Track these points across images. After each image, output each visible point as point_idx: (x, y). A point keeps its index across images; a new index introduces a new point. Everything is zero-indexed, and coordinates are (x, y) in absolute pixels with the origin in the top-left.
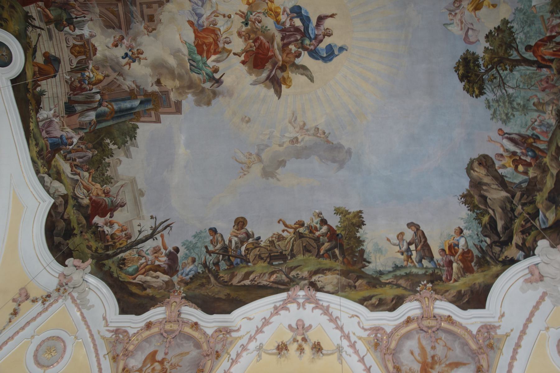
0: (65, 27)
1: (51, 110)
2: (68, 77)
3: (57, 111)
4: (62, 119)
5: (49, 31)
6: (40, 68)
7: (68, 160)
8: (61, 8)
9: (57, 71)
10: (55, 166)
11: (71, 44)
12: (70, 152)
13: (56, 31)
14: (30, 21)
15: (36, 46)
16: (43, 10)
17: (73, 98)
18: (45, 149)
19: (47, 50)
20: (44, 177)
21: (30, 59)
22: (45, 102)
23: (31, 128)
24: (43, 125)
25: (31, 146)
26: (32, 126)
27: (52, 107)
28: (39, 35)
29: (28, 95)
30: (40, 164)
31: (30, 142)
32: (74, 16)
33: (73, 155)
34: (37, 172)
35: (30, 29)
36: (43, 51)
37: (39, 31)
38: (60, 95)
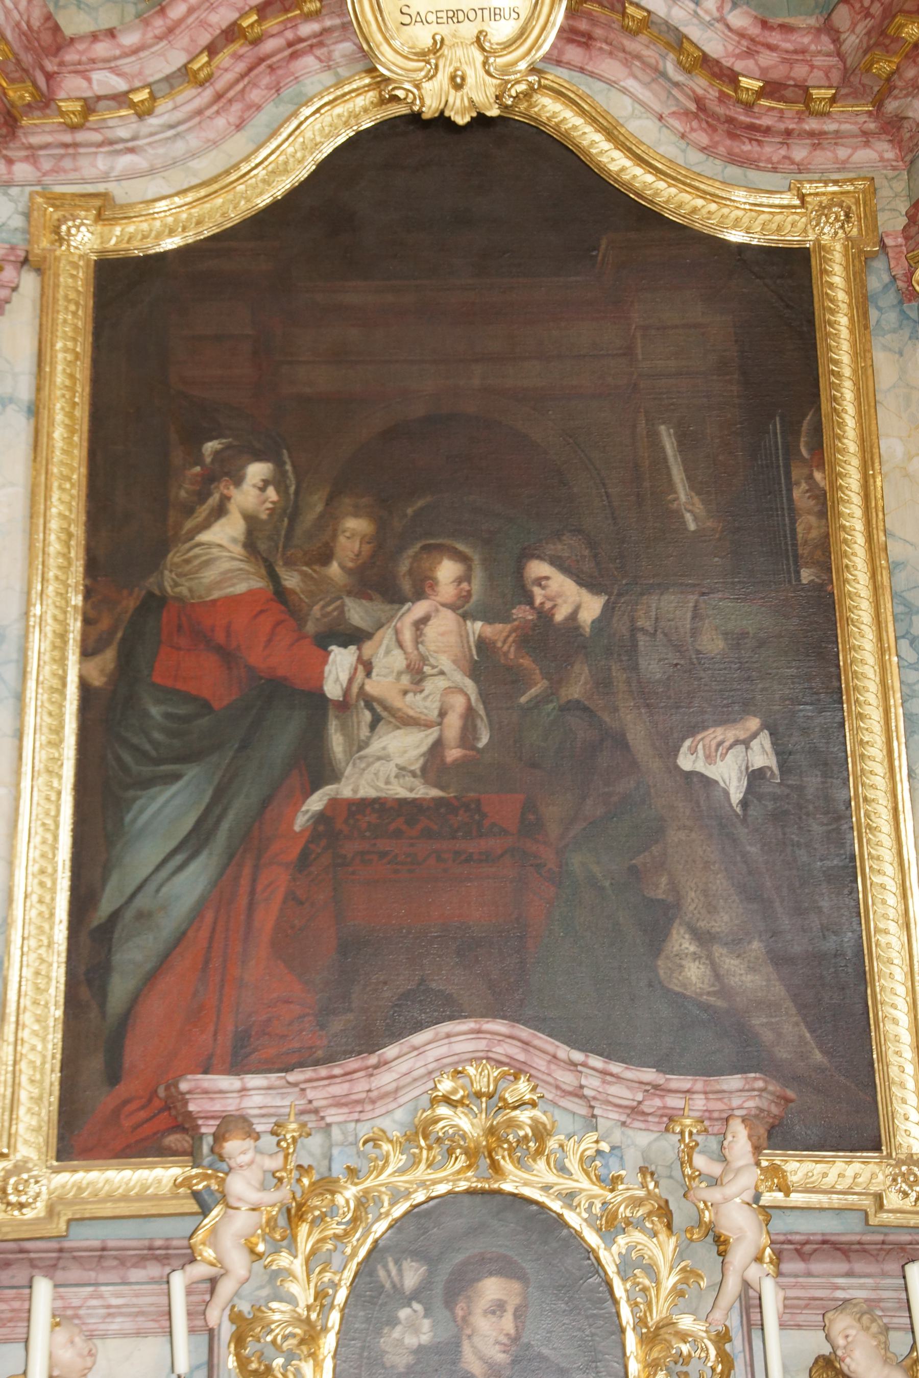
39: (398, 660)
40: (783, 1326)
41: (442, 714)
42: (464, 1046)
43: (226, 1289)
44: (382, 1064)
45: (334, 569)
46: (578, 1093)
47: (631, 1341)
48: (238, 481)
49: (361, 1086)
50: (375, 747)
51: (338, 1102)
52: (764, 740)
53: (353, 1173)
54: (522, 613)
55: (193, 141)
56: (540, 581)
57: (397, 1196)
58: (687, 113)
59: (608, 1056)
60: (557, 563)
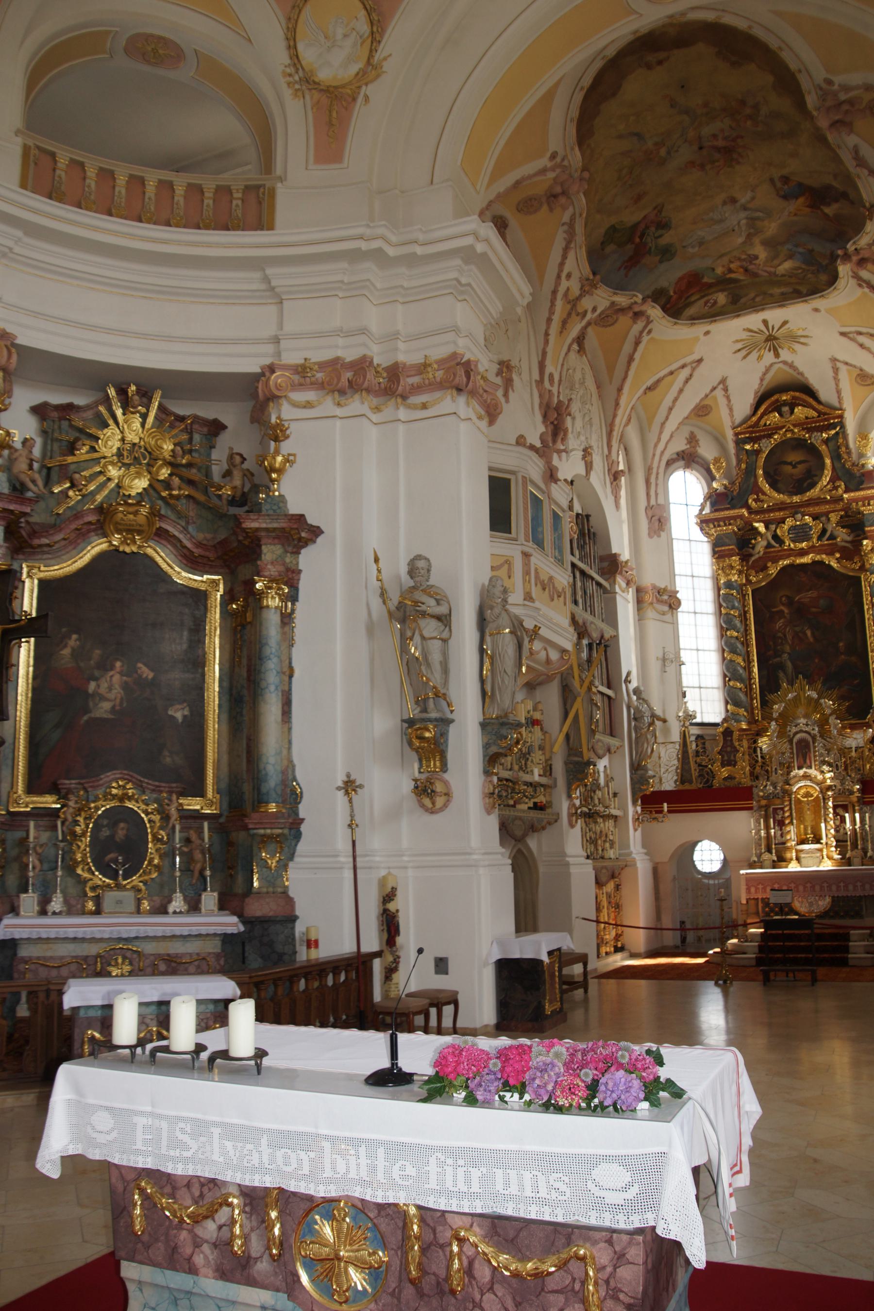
39: (106, 685)
40: (180, 832)
41: (115, 699)
42: (118, 776)
43: (67, 823)
44: (101, 779)
45: (92, 662)
46: (142, 786)
47: (150, 837)
48: (70, 638)
49: (96, 784)
50: (100, 705)
51: (91, 787)
52: (187, 708)
53: (94, 802)
54: (135, 675)
55: (63, 552)
56: (140, 668)
57: (103, 806)
58: (181, 556)
59: (148, 779)
60: (145, 665)
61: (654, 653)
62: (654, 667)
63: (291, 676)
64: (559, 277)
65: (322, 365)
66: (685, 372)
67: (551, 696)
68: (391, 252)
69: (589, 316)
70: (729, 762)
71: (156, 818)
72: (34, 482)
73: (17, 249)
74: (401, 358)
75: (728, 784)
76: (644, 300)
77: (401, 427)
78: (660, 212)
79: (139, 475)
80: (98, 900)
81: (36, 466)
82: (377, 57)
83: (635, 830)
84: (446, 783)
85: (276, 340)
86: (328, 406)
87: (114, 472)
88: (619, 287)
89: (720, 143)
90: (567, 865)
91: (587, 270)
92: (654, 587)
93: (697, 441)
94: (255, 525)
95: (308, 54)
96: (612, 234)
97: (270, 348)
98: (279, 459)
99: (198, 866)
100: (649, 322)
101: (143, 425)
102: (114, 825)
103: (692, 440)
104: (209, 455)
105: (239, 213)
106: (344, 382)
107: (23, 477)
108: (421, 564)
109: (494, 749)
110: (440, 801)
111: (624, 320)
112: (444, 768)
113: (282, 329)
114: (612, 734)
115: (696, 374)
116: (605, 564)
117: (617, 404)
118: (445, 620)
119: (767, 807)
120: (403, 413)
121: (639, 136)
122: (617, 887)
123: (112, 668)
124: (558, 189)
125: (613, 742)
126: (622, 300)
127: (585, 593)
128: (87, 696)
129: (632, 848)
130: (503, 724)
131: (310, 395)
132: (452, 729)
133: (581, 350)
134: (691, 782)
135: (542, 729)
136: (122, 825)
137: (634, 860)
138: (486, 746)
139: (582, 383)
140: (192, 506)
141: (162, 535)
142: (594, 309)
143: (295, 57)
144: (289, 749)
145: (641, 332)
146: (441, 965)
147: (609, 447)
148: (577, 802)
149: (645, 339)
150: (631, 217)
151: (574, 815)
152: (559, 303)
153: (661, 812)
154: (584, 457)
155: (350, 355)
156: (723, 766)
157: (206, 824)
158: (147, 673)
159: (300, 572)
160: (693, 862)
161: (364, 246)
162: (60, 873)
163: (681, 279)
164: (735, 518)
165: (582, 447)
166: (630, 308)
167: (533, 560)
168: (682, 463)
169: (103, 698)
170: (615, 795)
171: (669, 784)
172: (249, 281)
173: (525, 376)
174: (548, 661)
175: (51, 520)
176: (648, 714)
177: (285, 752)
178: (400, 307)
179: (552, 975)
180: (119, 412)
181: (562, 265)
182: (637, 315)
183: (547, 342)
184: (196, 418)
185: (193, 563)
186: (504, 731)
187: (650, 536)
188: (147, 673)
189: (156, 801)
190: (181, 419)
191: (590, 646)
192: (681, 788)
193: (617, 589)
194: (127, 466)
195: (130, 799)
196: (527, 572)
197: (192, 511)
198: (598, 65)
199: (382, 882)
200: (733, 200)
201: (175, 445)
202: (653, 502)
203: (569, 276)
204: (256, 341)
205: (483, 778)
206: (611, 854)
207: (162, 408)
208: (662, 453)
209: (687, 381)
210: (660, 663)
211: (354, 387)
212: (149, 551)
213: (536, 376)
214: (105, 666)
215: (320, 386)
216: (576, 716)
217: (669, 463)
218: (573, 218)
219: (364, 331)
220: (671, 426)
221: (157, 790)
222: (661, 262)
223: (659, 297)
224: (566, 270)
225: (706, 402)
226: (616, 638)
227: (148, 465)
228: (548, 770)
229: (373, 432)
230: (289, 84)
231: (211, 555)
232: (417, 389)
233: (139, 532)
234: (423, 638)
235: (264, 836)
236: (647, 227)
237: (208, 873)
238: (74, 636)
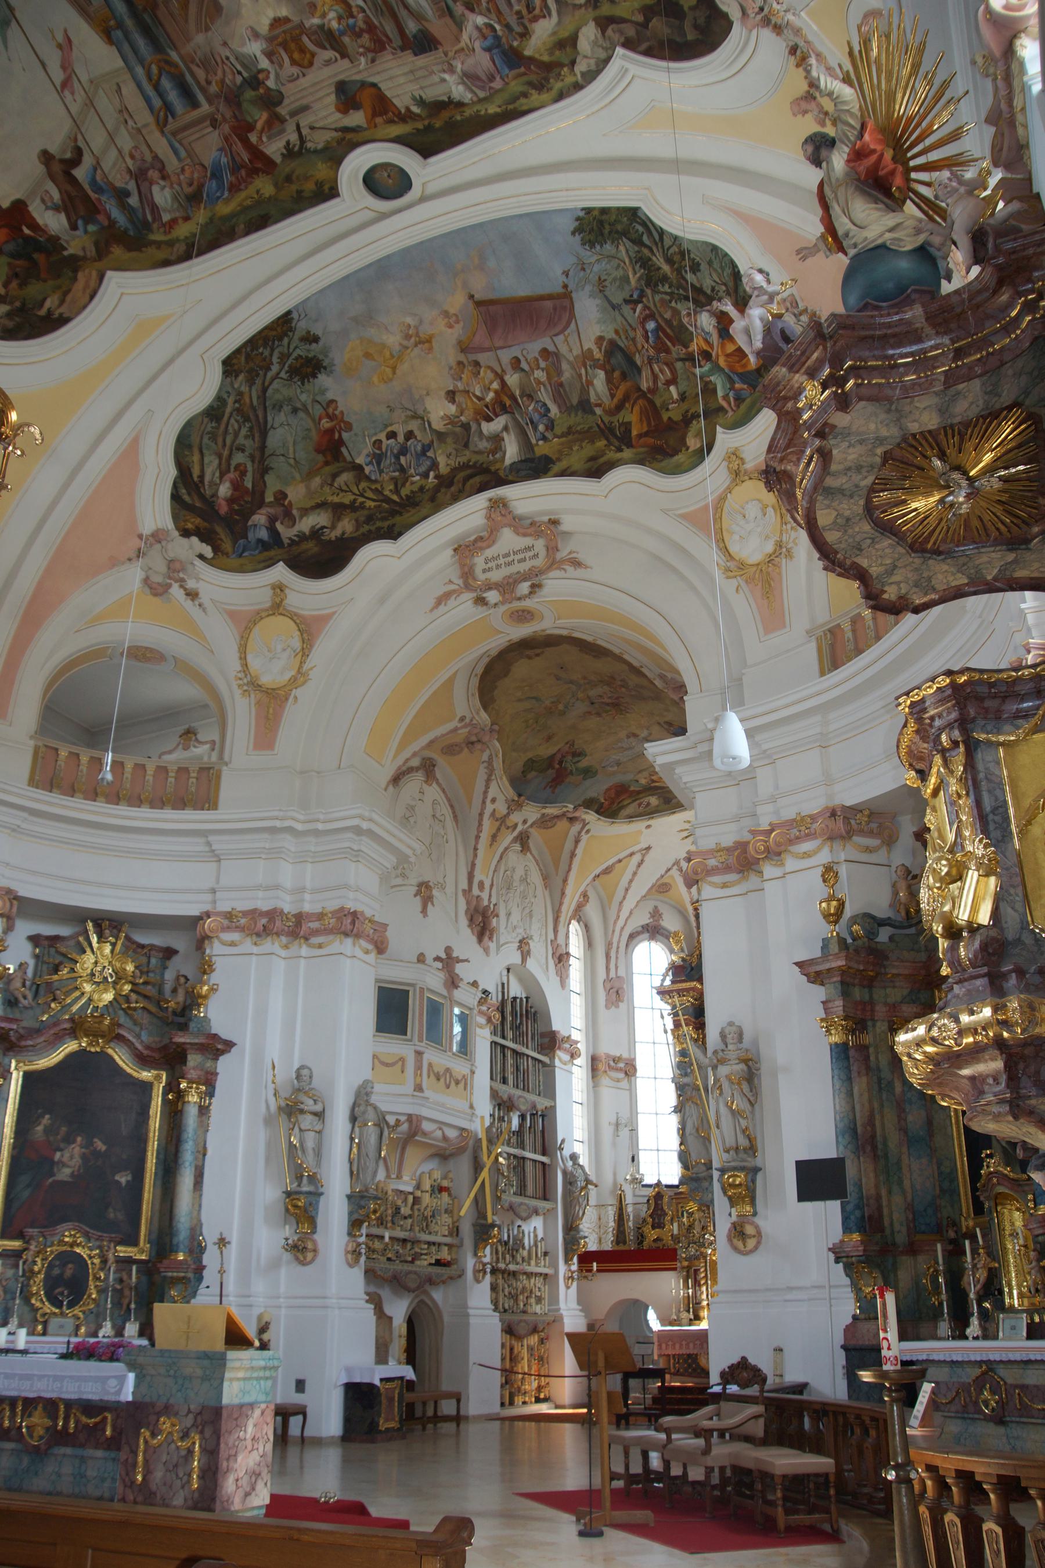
0: (269, 89)
1: (444, 80)
2: (363, 60)
3: (440, 67)
4: (451, 54)
5: (294, 114)
6: (375, 115)
7: (526, 28)
8: (239, 105)
9: (364, 84)
10: (551, 54)
11: (295, 70)
12: (508, 26)
13: (286, 102)
14: (296, 149)
15: (336, 130)
16: (262, 131)
17: (397, 42)
18: (525, 79)
19: (332, 109)
20: (583, 74)
21: (367, 134)
22: (433, 93)
23: (498, 110)
24: (482, 88)
25: (532, 106)
26: (493, 109)
27: (436, 79)
28: (312, 128)
29: (437, 125)
30: (558, 85)
31: (525, 108)
32: (239, 80)
33: (512, 20)
34: (578, 87)
35: (309, 145)
36: (338, 115)
37: (305, 131)
38: (406, 69)
61: (608, 1117)
62: (607, 1132)
63: (204, 1155)
64: (484, 802)
65: (245, 914)
66: (636, 858)
67: (463, 1166)
68: (299, 827)
69: (520, 828)
70: (658, 1225)
71: (97, 1261)
72: (25, 997)
73: (24, 825)
74: (307, 908)
75: (654, 1245)
76: (575, 808)
77: (302, 961)
78: (573, 745)
79: (106, 991)
80: (45, 1324)
81: (28, 983)
82: (305, 667)
83: (568, 1288)
84: (314, 1242)
85: (214, 891)
86: (248, 946)
87: (88, 988)
88: (548, 801)
89: (606, 700)
90: (468, 1315)
91: (511, 793)
92: (608, 1056)
93: (660, 915)
94: (182, 1040)
95: (255, 663)
96: (531, 765)
97: (209, 897)
98: (206, 988)
99: (126, 1301)
100: (585, 825)
101: (112, 951)
102: (64, 1265)
103: (656, 914)
104: (163, 974)
105: (193, 789)
106: (259, 927)
107: (16, 993)
108: (305, 1072)
109: (356, 1216)
110: (310, 1256)
111: (563, 824)
112: (314, 1232)
113: (218, 882)
114: (545, 1198)
115: (647, 859)
116: (546, 1040)
117: (563, 894)
118: (320, 1115)
119: (688, 1268)
120: (305, 951)
121: (536, 699)
122: (542, 1341)
123: (74, 1142)
124: (474, 739)
125: (547, 1205)
126: (552, 811)
127: (518, 1069)
128: (52, 1163)
129: (562, 1305)
130: (362, 1197)
131: (235, 936)
132: (322, 1199)
133: (525, 848)
134: (625, 1243)
135: (450, 1195)
136: (70, 1266)
137: (561, 1317)
138: (350, 1214)
139: (524, 880)
140: (146, 1015)
141: (119, 1038)
142: (525, 822)
143: (245, 665)
144: (199, 1210)
145: (580, 833)
146: (300, 1386)
147: (556, 931)
148: (487, 1260)
149: (584, 838)
150: (546, 751)
151: (479, 1272)
152: (487, 823)
153: (590, 1271)
154: (520, 947)
155: (265, 906)
156: (653, 1228)
157: (134, 1268)
158: (100, 1146)
159: (217, 1074)
160: (647, 1321)
161: (278, 824)
162: (17, 1301)
163: (608, 790)
164: (688, 990)
165: (520, 937)
166: (564, 815)
167: (425, 1056)
168: (647, 935)
169: (64, 1165)
170: (546, 1254)
171: (608, 1246)
172: (197, 845)
173: (450, 889)
174: (445, 1138)
175: (37, 1025)
176: (582, 1178)
177: (195, 1213)
178: (309, 865)
179: (391, 1400)
180: (94, 939)
181: (486, 793)
182: (572, 820)
183: (475, 856)
184: (152, 947)
185: (143, 1060)
186: (363, 1203)
187: (607, 1007)
188: (100, 1146)
189: (100, 1247)
190: (143, 946)
191: (523, 1117)
192: (617, 1248)
193: (557, 1062)
194: (98, 984)
195: (78, 1245)
196: (419, 1067)
197: (145, 1019)
198: (486, 660)
199: (260, 1317)
200: (635, 735)
201: (136, 967)
202: (612, 974)
203: (494, 800)
204: (200, 891)
205: (346, 1238)
206: (538, 1309)
207: (127, 938)
208: (622, 929)
209: (639, 865)
210: (612, 1129)
211: (266, 932)
212: (110, 1051)
213: (464, 884)
214: (69, 1140)
215: (241, 929)
216: (483, 1183)
217: (632, 936)
218: (490, 757)
219: (277, 887)
220: (629, 904)
221: (100, 1239)
222: (584, 779)
223: (589, 804)
224: (490, 797)
225: (665, 880)
226: (553, 1108)
227: (115, 983)
228: (455, 1231)
229: (280, 966)
230: (239, 686)
231: (156, 1055)
232: (316, 933)
233: (103, 1037)
234: (301, 1130)
235: (172, 1278)
236: (563, 757)
237: (133, 1306)
238: (47, 1116)
